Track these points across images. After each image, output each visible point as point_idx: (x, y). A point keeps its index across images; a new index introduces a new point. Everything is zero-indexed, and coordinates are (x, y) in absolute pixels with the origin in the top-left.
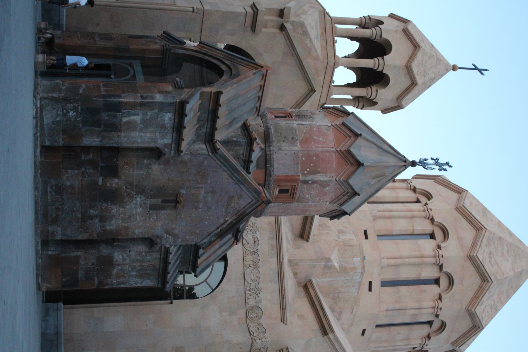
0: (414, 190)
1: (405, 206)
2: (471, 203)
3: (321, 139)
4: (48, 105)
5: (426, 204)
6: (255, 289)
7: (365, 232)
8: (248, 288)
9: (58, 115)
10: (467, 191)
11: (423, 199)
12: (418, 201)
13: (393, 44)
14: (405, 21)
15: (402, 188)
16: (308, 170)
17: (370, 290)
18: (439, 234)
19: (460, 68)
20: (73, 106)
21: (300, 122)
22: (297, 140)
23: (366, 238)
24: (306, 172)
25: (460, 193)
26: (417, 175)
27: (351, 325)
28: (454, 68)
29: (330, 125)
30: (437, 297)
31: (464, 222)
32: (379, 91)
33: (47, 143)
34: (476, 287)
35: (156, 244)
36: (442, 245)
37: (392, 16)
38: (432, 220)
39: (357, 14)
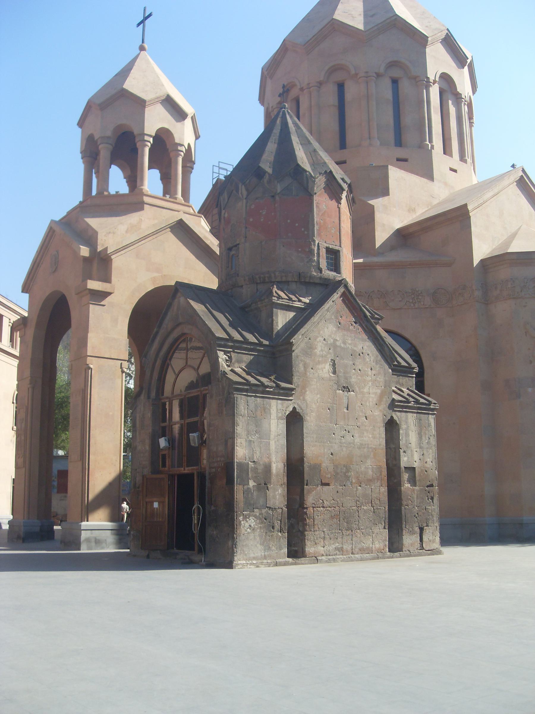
3: (264, 213)
4: (243, 550)
5: (302, 89)
6: (413, 296)
8: (412, 305)
9: (255, 538)
10: (284, 40)
11: (293, 93)
16: (303, 229)
17: (405, 160)
19: (143, 42)
20: (243, 520)
24: (306, 233)
26: (259, 99)
27: (446, 184)
32: (177, 141)
33: (286, 550)
35: (392, 417)
36: (353, 72)
37: (81, 124)
38: (320, 84)
39: (78, 167)
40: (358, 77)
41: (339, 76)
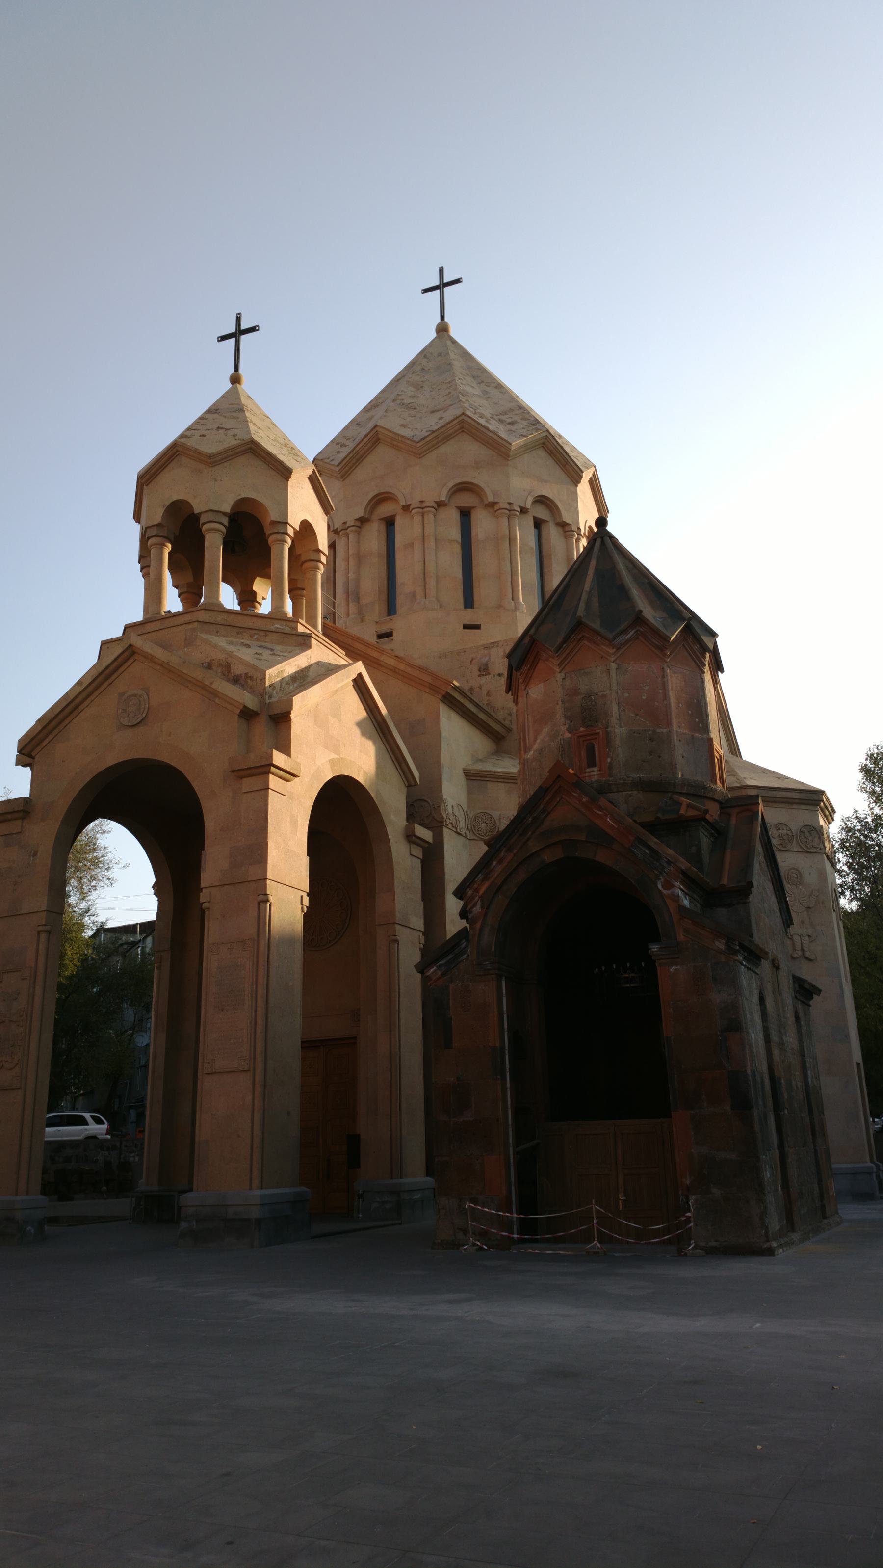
0: (362, 521)
1: (411, 545)
2: (404, 426)
3: (647, 688)
5: (406, 508)
7: (466, 627)
11: (386, 510)
12: (390, 523)
13: (244, 495)
14: (173, 454)
15: (358, 542)
18: (466, 500)
21: (614, 720)
22: (654, 731)
23: (477, 627)
25: (378, 439)
28: (235, 379)
29: (614, 666)
30: (560, 529)
31: (445, 449)
34: (550, 462)
36: (491, 499)
38: (440, 504)
40: (496, 508)
41: (466, 500)
